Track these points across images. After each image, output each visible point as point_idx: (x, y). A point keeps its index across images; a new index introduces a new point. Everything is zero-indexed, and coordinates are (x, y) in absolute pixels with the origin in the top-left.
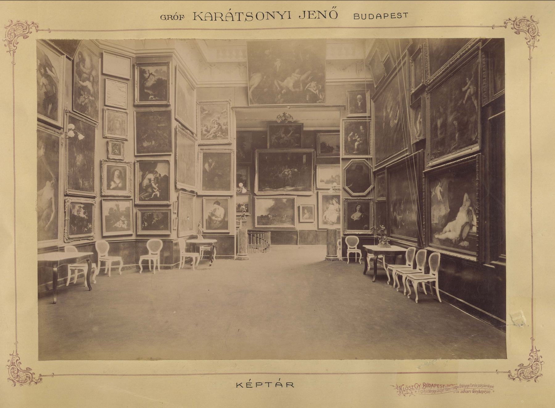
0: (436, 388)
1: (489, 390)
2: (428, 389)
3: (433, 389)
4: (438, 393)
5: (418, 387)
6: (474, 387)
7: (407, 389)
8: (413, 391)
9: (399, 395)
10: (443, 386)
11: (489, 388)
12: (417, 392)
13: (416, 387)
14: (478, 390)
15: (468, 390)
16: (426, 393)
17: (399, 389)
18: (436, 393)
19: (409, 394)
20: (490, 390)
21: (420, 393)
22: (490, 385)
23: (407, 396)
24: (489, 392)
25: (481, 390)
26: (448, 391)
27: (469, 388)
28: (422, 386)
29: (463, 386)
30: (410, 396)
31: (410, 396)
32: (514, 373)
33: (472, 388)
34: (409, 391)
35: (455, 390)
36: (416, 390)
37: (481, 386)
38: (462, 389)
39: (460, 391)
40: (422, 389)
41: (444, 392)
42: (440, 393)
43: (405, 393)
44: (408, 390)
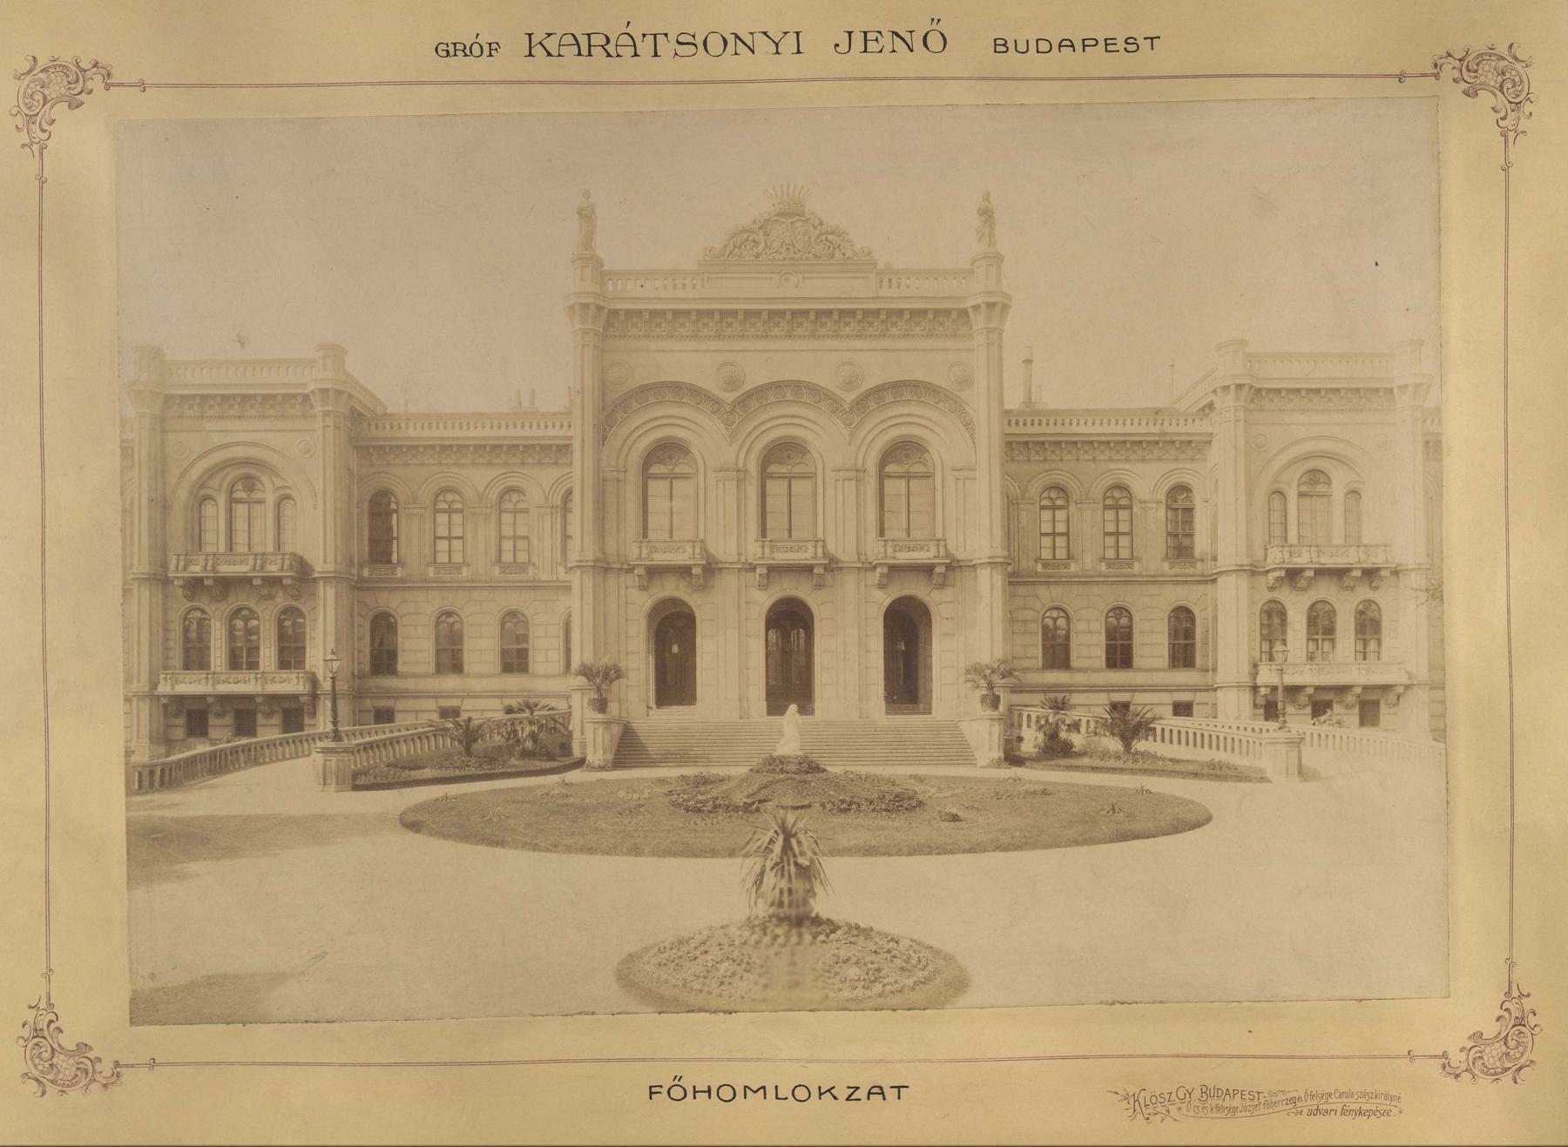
0: (1237, 1102)
1: (1387, 1108)
2: (1214, 1102)
3: (1228, 1102)
4: (1243, 1114)
5: (1188, 1095)
6: (1345, 1100)
7: (1154, 1100)
8: (1173, 1109)
9: (1132, 1118)
10: (1256, 1095)
11: (1388, 1102)
12: (1184, 1111)
13: (1182, 1097)
14: (1355, 1107)
15: (1329, 1107)
16: (1210, 1115)
17: (1131, 1101)
18: (1237, 1115)
19: (1159, 1117)
20: (1391, 1108)
21: (1193, 1114)
22: (1392, 1093)
23: (1156, 1119)
24: (1387, 1113)
25: (1364, 1107)
26: (1270, 1111)
27: (1330, 1101)
28: (1197, 1094)
29: (1312, 1096)
30: (1163, 1120)
31: (1163, 1120)
32: (1457, 1058)
33: (1338, 1100)
34: (1163, 1110)
35: (1290, 1106)
36: (1179, 1105)
37: (1364, 1095)
38: (1312, 1103)
39: (1305, 1110)
40: (1197, 1103)
41: (1256, 1113)
42: (1248, 1114)
43: (1148, 1111)
44: (1158, 1104)
